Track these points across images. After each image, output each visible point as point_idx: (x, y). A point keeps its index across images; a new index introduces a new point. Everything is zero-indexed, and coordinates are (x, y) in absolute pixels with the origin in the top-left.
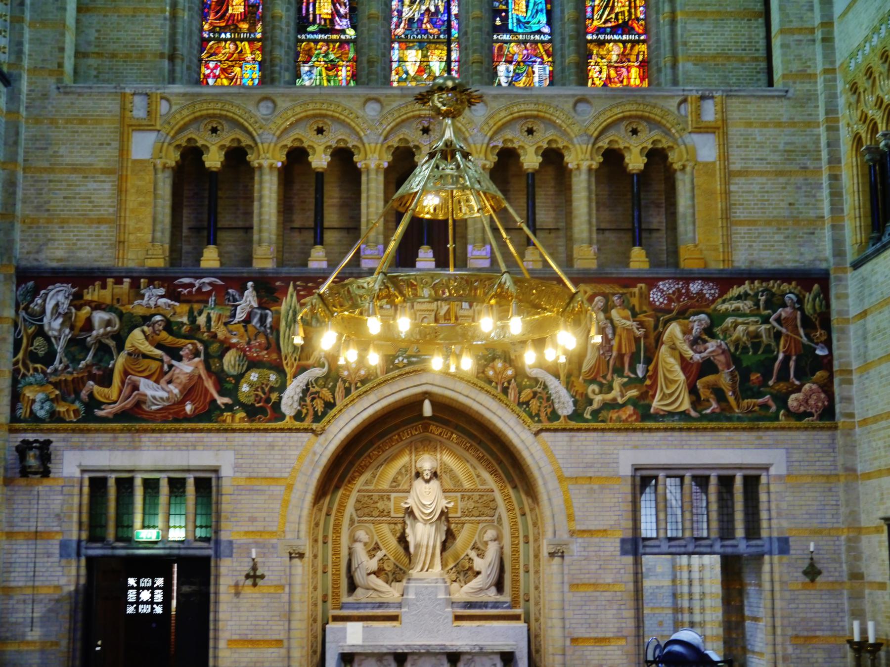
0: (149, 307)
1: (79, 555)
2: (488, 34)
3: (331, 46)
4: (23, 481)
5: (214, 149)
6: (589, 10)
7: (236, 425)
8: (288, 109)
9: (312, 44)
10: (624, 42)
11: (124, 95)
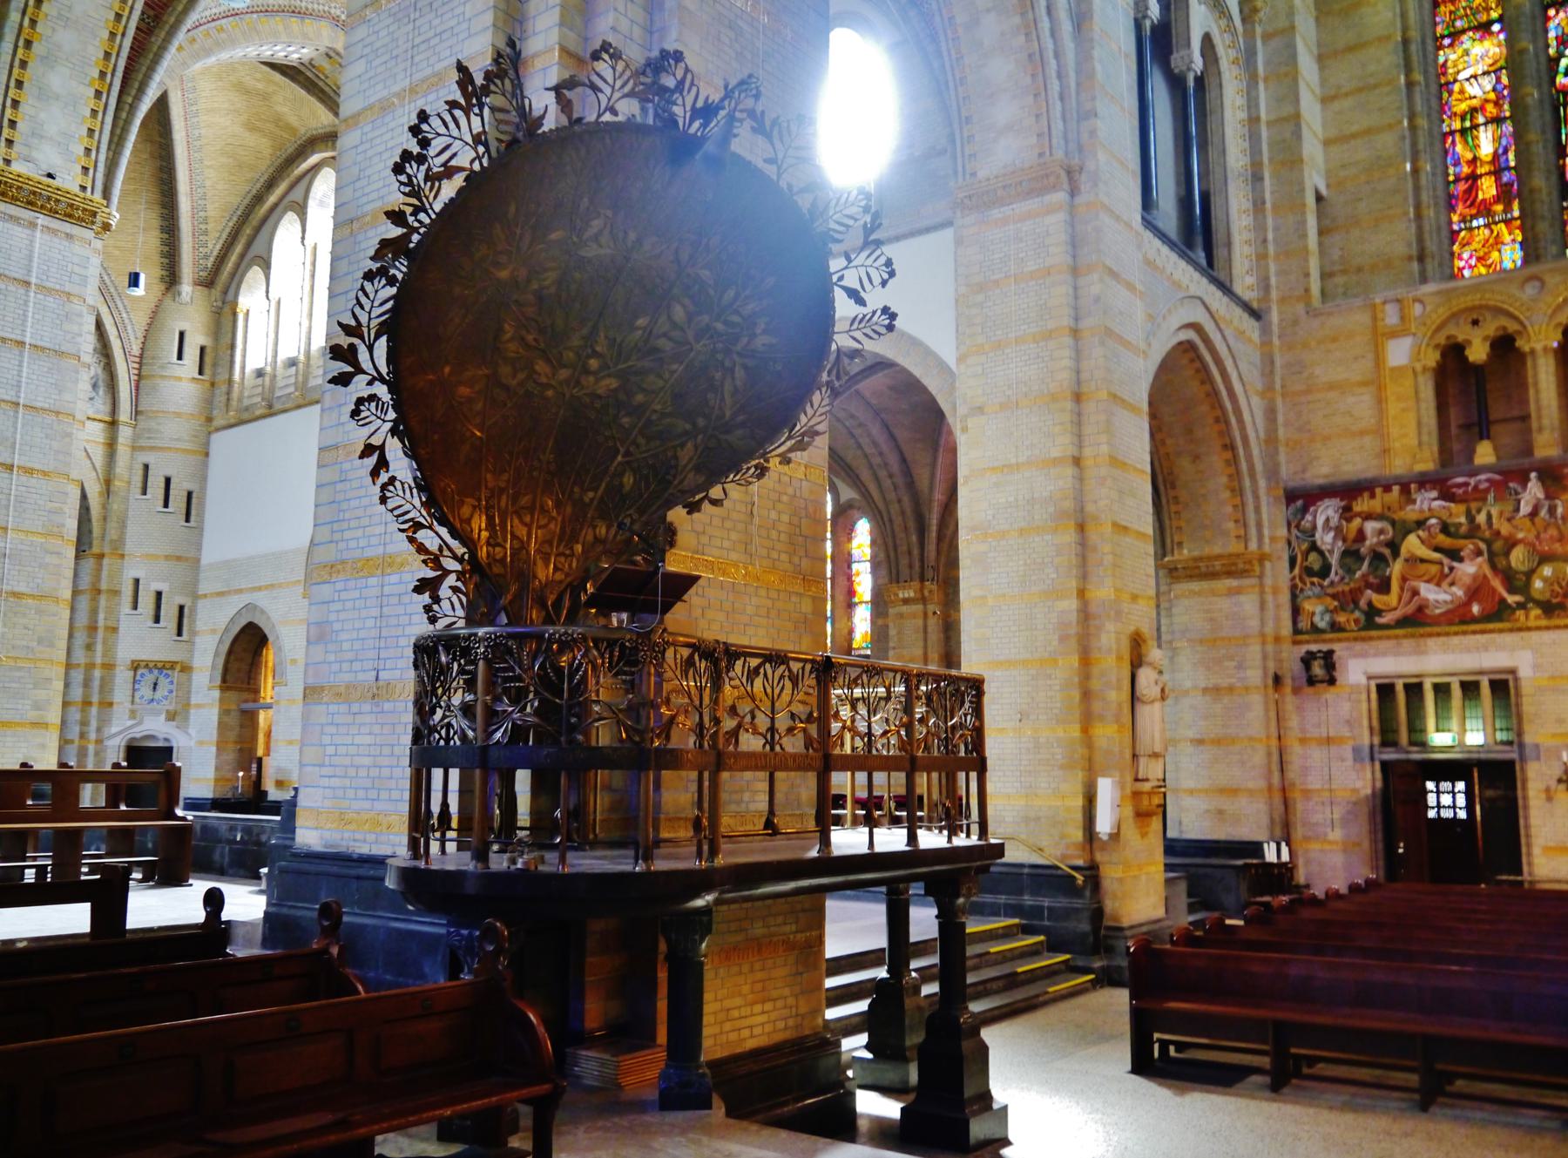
0: (1422, 511)
1: (1372, 759)
4: (1310, 690)
7: (1532, 623)
11: (1374, 306)
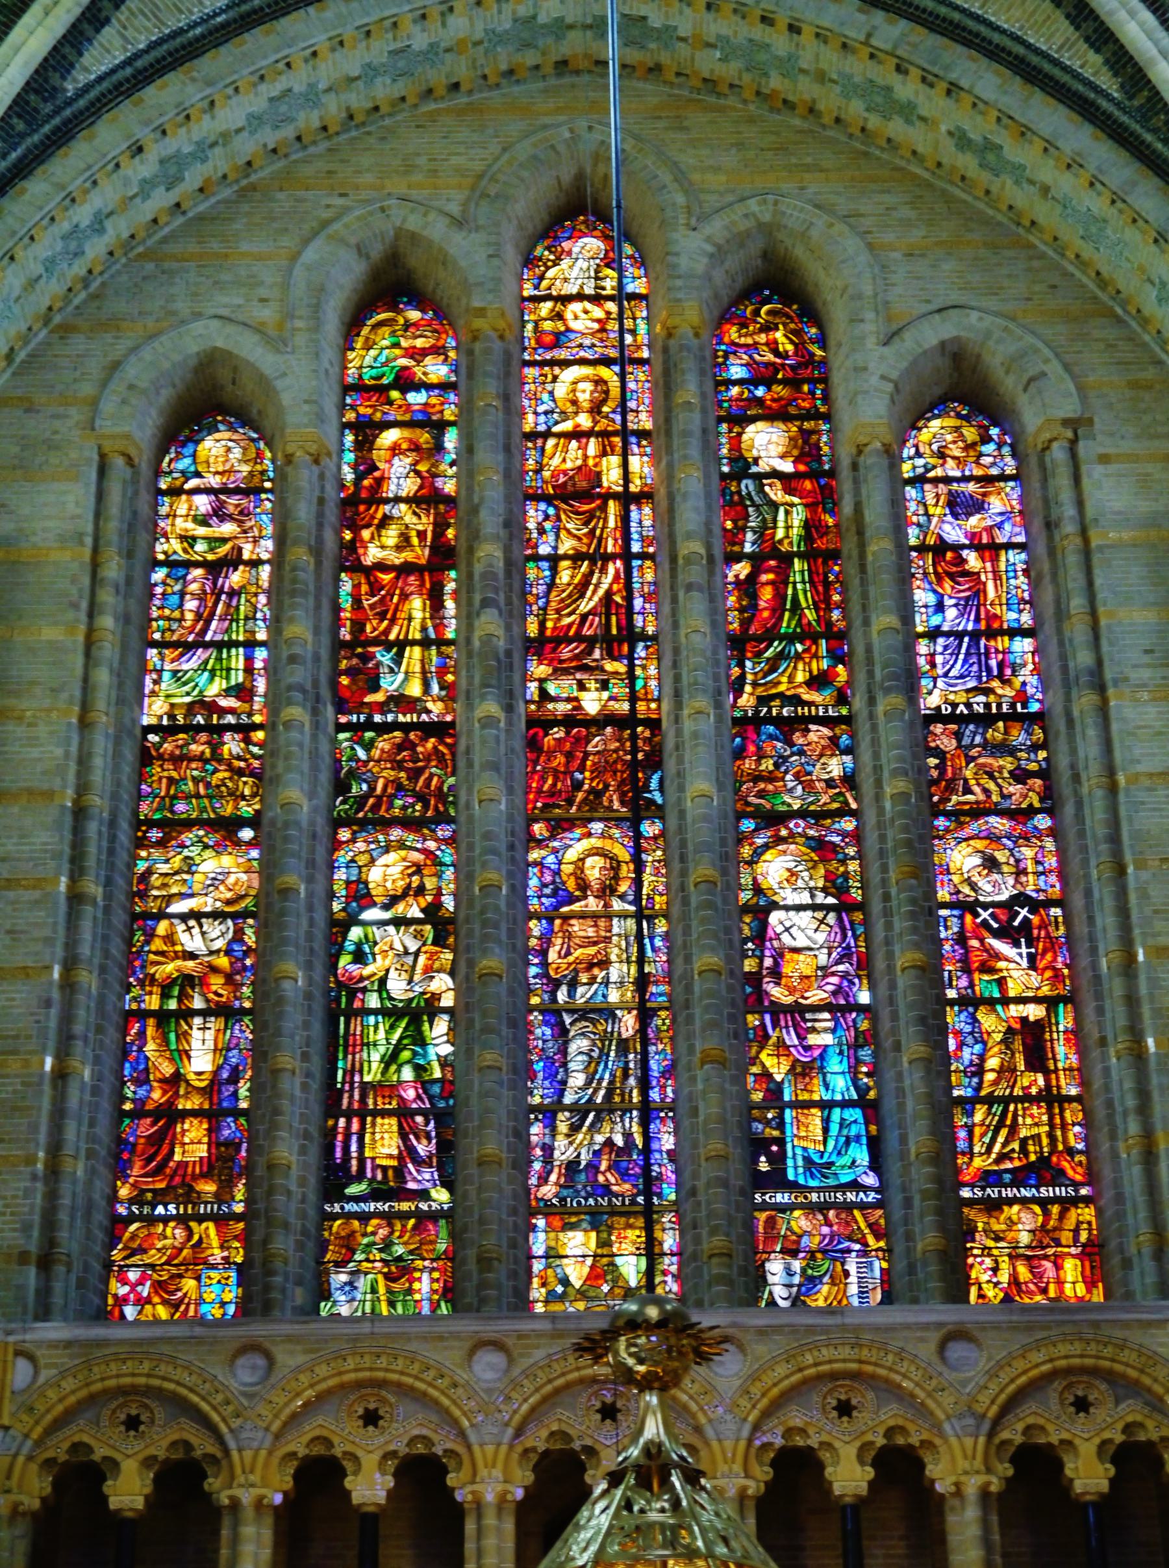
2: (742, 1192)
3: (398, 1227)
5: (129, 1467)
6: (962, 1134)
8: (300, 1372)
9: (356, 1223)
10: (1044, 1203)
